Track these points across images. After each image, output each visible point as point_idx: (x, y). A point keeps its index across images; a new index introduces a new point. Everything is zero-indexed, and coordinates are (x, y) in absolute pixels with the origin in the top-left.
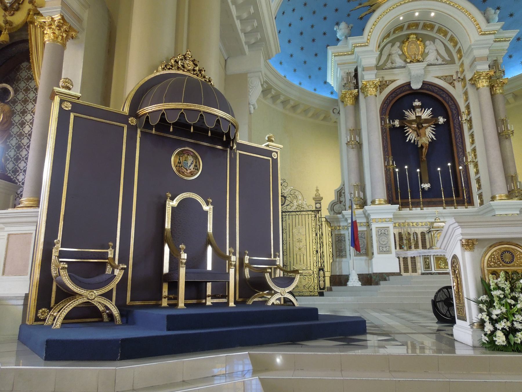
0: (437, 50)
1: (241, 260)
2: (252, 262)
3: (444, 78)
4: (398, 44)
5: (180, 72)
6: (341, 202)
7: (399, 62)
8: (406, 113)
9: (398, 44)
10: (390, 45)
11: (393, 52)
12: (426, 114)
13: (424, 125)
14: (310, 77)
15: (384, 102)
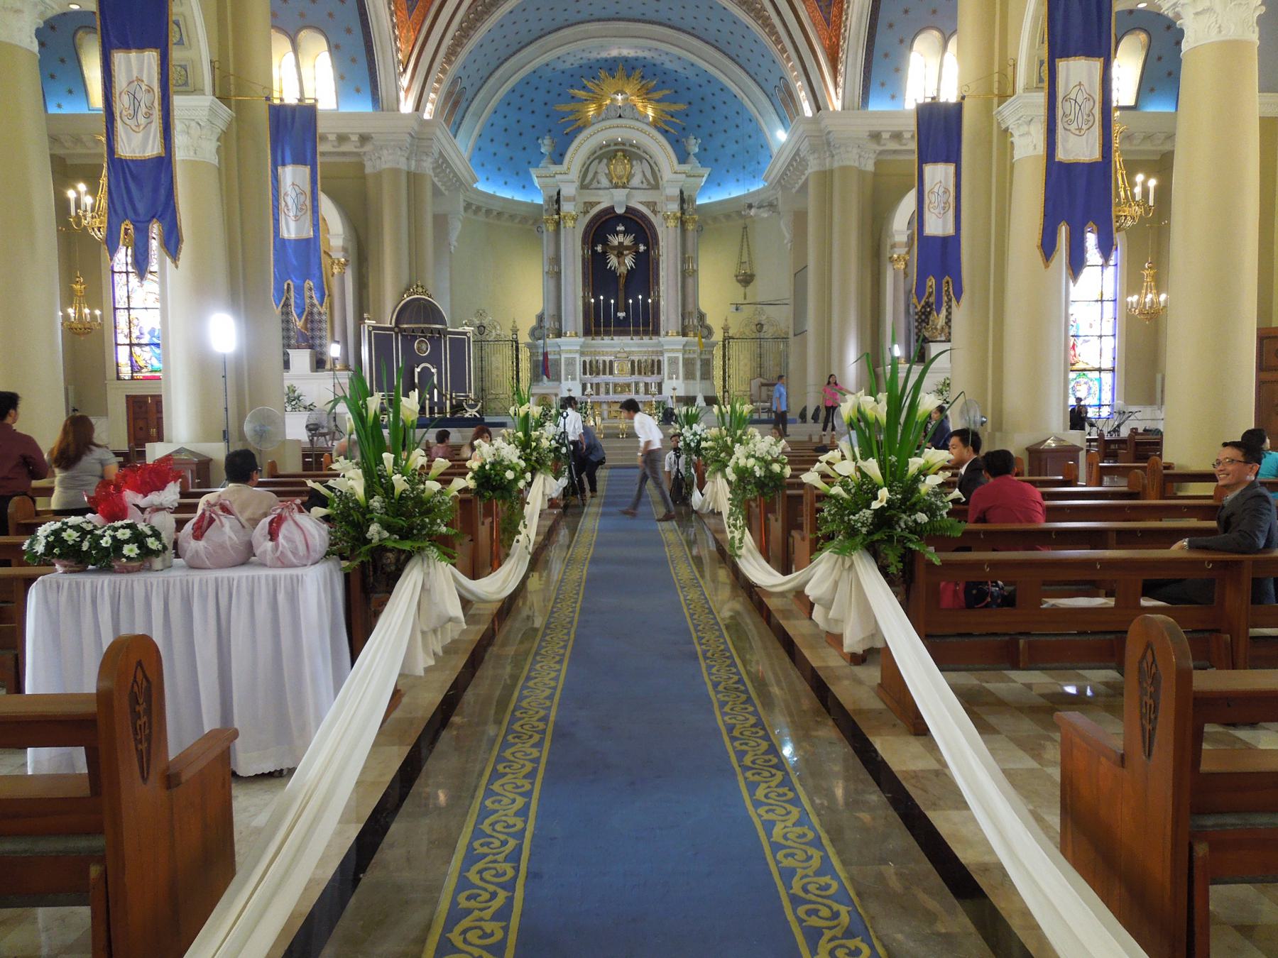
0: (643, 172)
1: (451, 395)
2: (456, 396)
3: (647, 204)
4: (605, 161)
5: (416, 296)
6: (541, 327)
7: (605, 182)
8: (609, 237)
9: (605, 161)
10: (597, 161)
11: (599, 171)
12: (628, 241)
13: (625, 252)
14: (517, 174)
15: (588, 226)
